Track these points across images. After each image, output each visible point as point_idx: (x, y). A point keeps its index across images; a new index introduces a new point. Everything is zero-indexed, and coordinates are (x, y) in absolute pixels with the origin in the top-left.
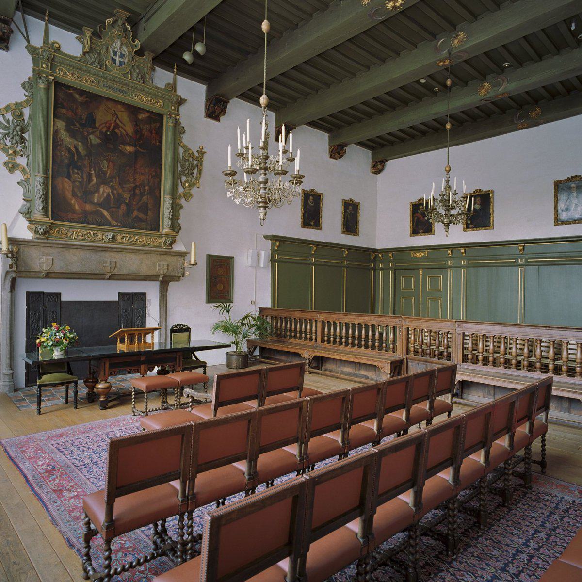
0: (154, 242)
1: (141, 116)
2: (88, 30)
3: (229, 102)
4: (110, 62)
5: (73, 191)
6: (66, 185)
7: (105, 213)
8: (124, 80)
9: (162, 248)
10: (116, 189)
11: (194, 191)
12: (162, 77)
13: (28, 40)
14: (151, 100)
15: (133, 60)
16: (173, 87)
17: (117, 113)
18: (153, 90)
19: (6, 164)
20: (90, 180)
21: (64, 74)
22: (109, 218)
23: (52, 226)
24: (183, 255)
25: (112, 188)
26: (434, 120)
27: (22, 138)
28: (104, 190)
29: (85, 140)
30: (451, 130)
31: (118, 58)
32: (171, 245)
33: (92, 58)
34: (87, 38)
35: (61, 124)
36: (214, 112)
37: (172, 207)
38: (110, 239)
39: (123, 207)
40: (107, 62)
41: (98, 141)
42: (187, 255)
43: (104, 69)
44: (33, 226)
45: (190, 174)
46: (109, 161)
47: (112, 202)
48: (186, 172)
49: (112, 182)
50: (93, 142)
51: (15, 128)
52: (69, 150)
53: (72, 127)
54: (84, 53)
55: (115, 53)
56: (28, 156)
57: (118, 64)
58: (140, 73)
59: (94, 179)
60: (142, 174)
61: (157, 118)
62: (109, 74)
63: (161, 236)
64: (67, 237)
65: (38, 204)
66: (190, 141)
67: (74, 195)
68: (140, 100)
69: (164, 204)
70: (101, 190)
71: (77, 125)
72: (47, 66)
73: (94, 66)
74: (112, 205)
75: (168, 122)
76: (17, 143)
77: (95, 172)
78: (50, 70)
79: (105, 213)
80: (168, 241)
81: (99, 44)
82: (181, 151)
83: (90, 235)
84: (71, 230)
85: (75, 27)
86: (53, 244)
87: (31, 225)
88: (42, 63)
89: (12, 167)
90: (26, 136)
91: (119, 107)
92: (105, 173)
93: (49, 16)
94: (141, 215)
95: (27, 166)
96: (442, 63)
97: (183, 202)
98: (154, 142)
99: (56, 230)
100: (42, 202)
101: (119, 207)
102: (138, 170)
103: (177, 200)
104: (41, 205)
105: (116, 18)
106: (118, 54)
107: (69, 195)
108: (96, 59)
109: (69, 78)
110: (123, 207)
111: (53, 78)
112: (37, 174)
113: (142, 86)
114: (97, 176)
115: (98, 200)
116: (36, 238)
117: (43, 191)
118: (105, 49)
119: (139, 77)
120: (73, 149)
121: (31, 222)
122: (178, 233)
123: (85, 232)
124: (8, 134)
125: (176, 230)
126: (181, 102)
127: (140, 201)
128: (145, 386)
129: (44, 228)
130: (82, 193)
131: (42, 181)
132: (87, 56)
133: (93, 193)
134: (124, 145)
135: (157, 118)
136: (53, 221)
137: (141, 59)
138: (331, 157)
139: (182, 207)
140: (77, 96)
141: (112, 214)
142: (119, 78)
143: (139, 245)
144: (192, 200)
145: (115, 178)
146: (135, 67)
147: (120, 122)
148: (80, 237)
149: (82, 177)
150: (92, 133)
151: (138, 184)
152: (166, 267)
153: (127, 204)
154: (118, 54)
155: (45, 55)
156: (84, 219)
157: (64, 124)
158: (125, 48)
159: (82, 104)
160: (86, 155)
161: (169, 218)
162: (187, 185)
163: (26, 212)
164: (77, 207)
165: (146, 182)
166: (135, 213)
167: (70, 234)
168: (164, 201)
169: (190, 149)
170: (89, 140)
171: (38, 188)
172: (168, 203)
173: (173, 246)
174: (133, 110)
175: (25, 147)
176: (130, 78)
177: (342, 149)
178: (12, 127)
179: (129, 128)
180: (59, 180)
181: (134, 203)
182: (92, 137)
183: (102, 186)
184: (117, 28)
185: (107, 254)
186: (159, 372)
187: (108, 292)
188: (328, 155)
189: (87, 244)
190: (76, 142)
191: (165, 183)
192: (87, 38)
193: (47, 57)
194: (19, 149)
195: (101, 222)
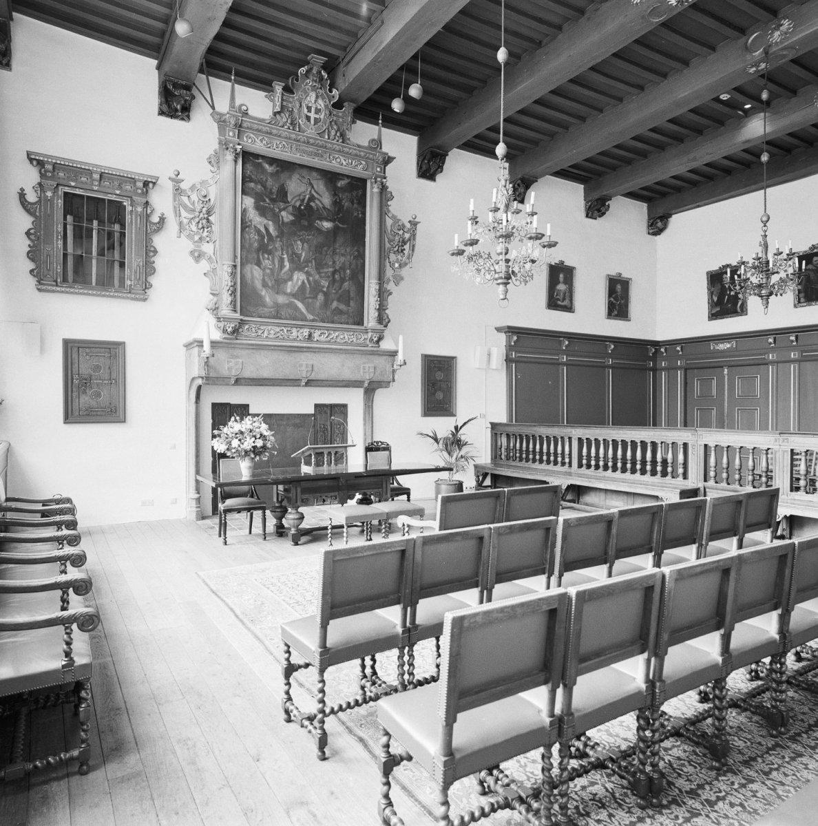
1: (340, 184)
3: (447, 155)
4: (304, 120)
5: (263, 280)
7: (300, 305)
8: (321, 141)
11: (405, 272)
12: (363, 132)
13: (213, 107)
15: (330, 115)
16: (377, 143)
19: (192, 253)
20: (282, 266)
22: (304, 310)
23: (242, 323)
24: (394, 354)
25: (308, 274)
26: (744, 151)
29: (276, 218)
30: (768, 162)
31: (312, 115)
32: (378, 342)
33: (284, 118)
35: (249, 202)
36: (428, 170)
37: (379, 294)
41: (291, 218)
44: (222, 325)
46: (303, 241)
47: (308, 292)
48: (396, 249)
49: (307, 266)
50: (286, 220)
52: (258, 231)
54: (275, 114)
57: (312, 121)
58: (338, 130)
59: (287, 264)
60: (343, 255)
61: (358, 185)
65: (226, 298)
66: (401, 209)
67: (265, 285)
68: (339, 164)
70: (295, 277)
71: (267, 200)
74: (308, 296)
75: (372, 188)
79: (300, 305)
82: (389, 222)
85: (264, 84)
86: (243, 344)
88: (229, 131)
89: (198, 256)
91: (315, 174)
92: (299, 257)
93: (236, 75)
94: (342, 307)
96: (754, 69)
97: (391, 286)
98: (356, 214)
100: (231, 295)
101: (315, 297)
104: (230, 299)
106: (313, 110)
107: (258, 284)
109: (257, 145)
110: (321, 297)
114: (291, 261)
116: (225, 338)
118: (298, 105)
120: (263, 230)
121: (219, 319)
122: (386, 326)
123: (278, 329)
126: (388, 160)
127: (340, 288)
128: (344, 517)
130: (273, 282)
132: (278, 116)
133: (286, 281)
135: (358, 185)
136: (242, 317)
137: (340, 113)
138: (587, 216)
139: (391, 294)
140: (267, 166)
142: (315, 139)
143: (340, 344)
144: (402, 283)
145: (311, 262)
147: (317, 193)
148: (271, 336)
149: (273, 262)
150: (284, 209)
151: (337, 268)
153: (326, 294)
154: (313, 110)
158: (320, 101)
159: (272, 175)
160: (277, 237)
164: (268, 299)
165: (347, 263)
166: (335, 304)
168: (369, 287)
171: (226, 280)
174: (330, 177)
176: (327, 137)
177: (604, 205)
178: (198, 210)
179: (326, 200)
180: (248, 268)
182: (283, 213)
184: (311, 77)
186: (361, 502)
187: (301, 403)
188: (584, 214)
189: (280, 344)
190: (266, 221)
191: (370, 264)
194: (205, 234)
195: (296, 316)
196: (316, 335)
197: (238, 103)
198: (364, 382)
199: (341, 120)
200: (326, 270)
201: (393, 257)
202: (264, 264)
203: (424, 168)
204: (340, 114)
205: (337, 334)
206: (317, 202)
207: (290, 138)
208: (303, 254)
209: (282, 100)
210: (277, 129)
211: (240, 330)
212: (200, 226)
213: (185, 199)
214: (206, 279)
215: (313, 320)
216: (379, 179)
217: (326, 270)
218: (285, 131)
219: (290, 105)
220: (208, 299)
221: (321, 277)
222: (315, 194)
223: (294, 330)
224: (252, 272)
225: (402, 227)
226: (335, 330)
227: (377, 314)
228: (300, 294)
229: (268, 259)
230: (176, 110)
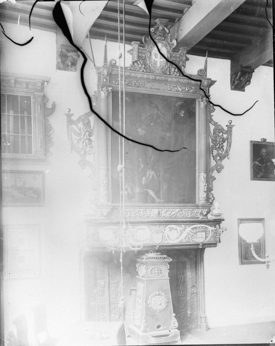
7: (151, 193)
14: (185, 88)
16: (203, 72)
17: (158, 106)
22: (154, 196)
27: (90, 140)
34: (136, 50)
37: (207, 181)
38: (157, 215)
40: (150, 65)
41: (144, 132)
42: (222, 222)
45: (220, 147)
48: (217, 147)
50: (140, 134)
51: (85, 133)
54: (133, 63)
56: (94, 154)
70: (148, 173)
72: (106, 79)
76: (86, 145)
80: (204, 212)
81: (144, 51)
82: (212, 127)
95: (94, 162)
97: (215, 174)
99: (116, 212)
100: (106, 190)
108: (142, 65)
111: (111, 88)
117: (106, 181)
124: (80, 139)
125: (210, 201)
129: (108, 211)
131: (105, 173)
132: (135, 64)
139: (215, 179)
141: (157, 193)
144: (223, 171)
155: (106, 73)
169: (220, 125)
172: (203, 177)
175: (91, 147)
176: (168, 73)
178: (83, 133)
194: (88, 149)
197: (109, 59)
203: (236, 83)
204: (178, 56)
208: (153, 157)
209: (138, 52)
212: (85, 144)
218: (139, 74)
219: (144, 55)
223: (148, 210)
225: (221, 130)
227: (205, 195)
230: (68, 66)
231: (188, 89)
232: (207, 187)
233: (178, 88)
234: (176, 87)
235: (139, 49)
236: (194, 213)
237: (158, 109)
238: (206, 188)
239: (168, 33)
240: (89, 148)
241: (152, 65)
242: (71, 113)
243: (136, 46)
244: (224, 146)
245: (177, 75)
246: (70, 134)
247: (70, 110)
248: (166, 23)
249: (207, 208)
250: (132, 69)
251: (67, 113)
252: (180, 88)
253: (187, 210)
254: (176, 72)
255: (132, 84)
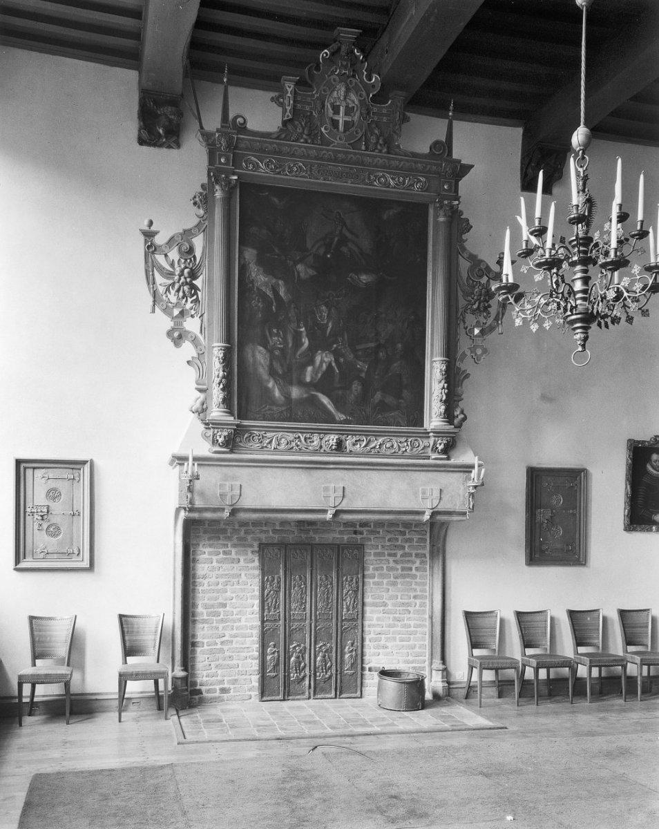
0: (413, 447)
2: (290, 81)
4: (329, 126)
6: (259, 357)
7: (325, 400)
9: (428, 458)
10: (343, 355)
14: (404, 181)
15: (368, 113)
18: (407, 161)
19: (169, 334)
20: (297, 343)
21: (253, 167)
22: (331, 407)
25: (337, 354)
27: (193, 287)
28: (323, 359)
29: (287, 274)
31: (341, 118)
34: (289, 95)
35: (250, 254)
38: (334, 447)
39: (356, 387)
40: (323, 129)
41: (311, 272)
43: (319, 142)
44: (210, 433)
47: (337, 379)
48: (475, 307)
50: (302, 275)
51: (182, 271)
52: (263, 296)
53: (268, 255)
54: (285, 123)
55: (336, 110)
56: (202, 315)
57: (341, 127)
58: (381, 134)
59: (306, 342)
62: (328, 150)
63: (426, 435)
64: (263, 447)
65: (217, 394)
67: (272, 373)
68: (386, 184)
69: (431, 374)
70: (318, 359)
72: (227, 159)
73: (302, 140)
75: (436, 216)
77: (306, 329)
78: (233, 166)
79: (325, 400)
80: (440, 444)
81: (309, 99)
82: (464, 265)
83: (300, 441)
84: (269, 435)
87: (208, 431)
90: (198, 283)
94: (390, 400)
97: (466, 365)
100: (223, 390)
101: (347, 387)
102: (384, 315)
103: (457, 364)
104: (221, 396)
105: (335, 46)
107: (263, 372)
108: (303, 129)
109: (263, 171)
110: (356, 387)
111: (236, 177)
112: (215, 344)
113: (389, 159)
114: (311, 336)
115: (312, 377)
116: (216, 452)
117: (224, 371)
119: (381, 141)
120: (270, 293)
122: (459, 426)
123: (291, 436)
124: (173, 284)
125: (456, 421)
129: (226, 434)
132: (290, 127)
133: (303, 367)
134: (357, 274)
135: (414, 214)
136: (237, 422)
139: (467, 376)
140: (276, 200)
142: (346, 153)
146: (374, 126)
147: (352, 233)
149: (285, 339)
150: (301, 261)
151: (382, 341)
152: (436, 494)
156: (291, 413)
157: (255, 252)
158: (353, 96)
161: (441, 401)
162: (477, 331)
163: (200, 410)
164: (277, 393)
166: (378, 396)
167: (268, 440)
169: (482, 261)
170: (296, 273)
171: (217, 369)
172: (439, 370)
173: (452, 453)
174: (371, 206)
175: (197, 301)
176: (363, 148)
179: (366, 244)
180: (248, 351)
181: (376, 377)
182: (300, 267)
183: (319, 352)
185: (331, 474)
190: (274, 281)
191: (432, 334)
192: (289, 95)
193: (230, 145)
194: (189, 305)
196: (349, 443)
197: (231, 116)
198: (423, 513)
199: (385, 120)
200: (362, 346)
201: (470, 319)
202: (271, 343)
204: (384, 111)
205: (381, 440)
206: (350, 245)
207: (308, 157)
208: (330, 324)
209: (294, 101)
210: (286, 145)
211: (238, 440)
212: (181, 294)
213: (160, 259)
214: (191, 369)
215: (346, 422)
216: (446, 202)
217: (362, 346)
220: (193, 398)
221: (357, 357)
222: (348, 234)
223: (316, 438)
224: (253, 356)
226: (377, 434)
228: (325, 383)
229: (278, 335)
231: (411, 182)
232: (446, 391)
233: (386, 180)
234: (383, 176)
235: (295, 93)
236: (418, 446)
237: (344, 224)
238: (446, 394)
239: (362, 62)
240: (191, 302)
241: (326, 129)
242: (153, 228)
243: (290, 87)
244: (489, 306)
245: (384, 151)
246: (151, 273)
247: (151, 223)
248: (356, 38)
249: (447, 437)
250: (283, 136)
251: (147, 228)
252: (392, 179)
253: (403, 440)
254: (381, 145)
255: (284, 171)
